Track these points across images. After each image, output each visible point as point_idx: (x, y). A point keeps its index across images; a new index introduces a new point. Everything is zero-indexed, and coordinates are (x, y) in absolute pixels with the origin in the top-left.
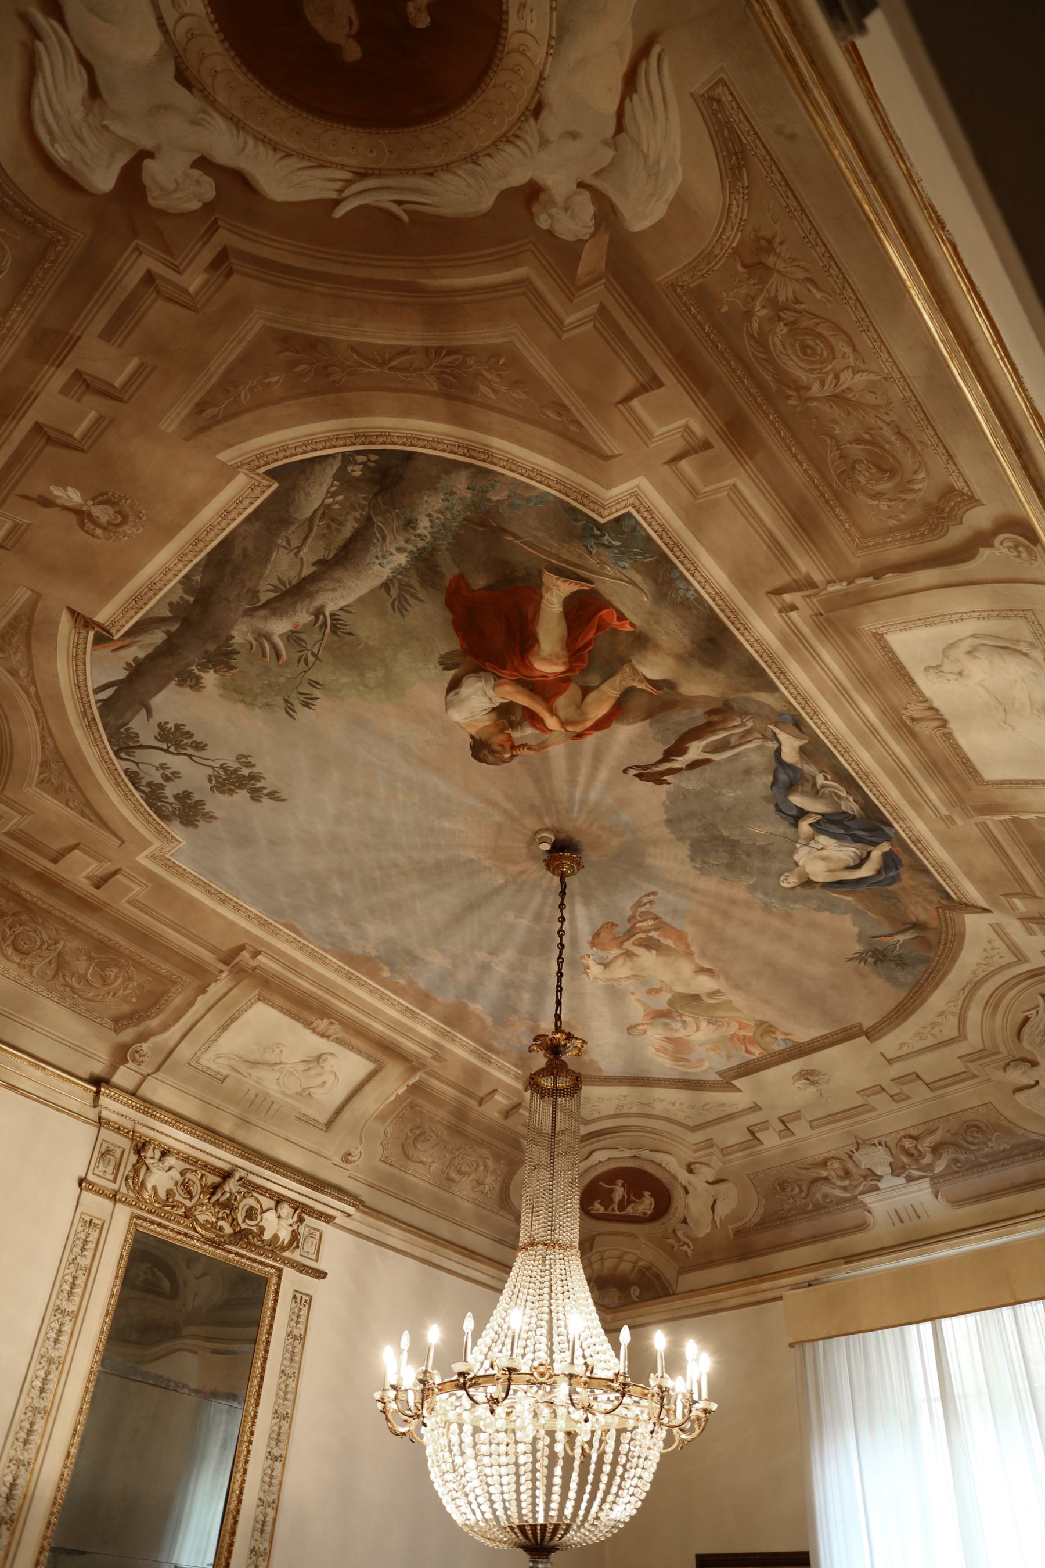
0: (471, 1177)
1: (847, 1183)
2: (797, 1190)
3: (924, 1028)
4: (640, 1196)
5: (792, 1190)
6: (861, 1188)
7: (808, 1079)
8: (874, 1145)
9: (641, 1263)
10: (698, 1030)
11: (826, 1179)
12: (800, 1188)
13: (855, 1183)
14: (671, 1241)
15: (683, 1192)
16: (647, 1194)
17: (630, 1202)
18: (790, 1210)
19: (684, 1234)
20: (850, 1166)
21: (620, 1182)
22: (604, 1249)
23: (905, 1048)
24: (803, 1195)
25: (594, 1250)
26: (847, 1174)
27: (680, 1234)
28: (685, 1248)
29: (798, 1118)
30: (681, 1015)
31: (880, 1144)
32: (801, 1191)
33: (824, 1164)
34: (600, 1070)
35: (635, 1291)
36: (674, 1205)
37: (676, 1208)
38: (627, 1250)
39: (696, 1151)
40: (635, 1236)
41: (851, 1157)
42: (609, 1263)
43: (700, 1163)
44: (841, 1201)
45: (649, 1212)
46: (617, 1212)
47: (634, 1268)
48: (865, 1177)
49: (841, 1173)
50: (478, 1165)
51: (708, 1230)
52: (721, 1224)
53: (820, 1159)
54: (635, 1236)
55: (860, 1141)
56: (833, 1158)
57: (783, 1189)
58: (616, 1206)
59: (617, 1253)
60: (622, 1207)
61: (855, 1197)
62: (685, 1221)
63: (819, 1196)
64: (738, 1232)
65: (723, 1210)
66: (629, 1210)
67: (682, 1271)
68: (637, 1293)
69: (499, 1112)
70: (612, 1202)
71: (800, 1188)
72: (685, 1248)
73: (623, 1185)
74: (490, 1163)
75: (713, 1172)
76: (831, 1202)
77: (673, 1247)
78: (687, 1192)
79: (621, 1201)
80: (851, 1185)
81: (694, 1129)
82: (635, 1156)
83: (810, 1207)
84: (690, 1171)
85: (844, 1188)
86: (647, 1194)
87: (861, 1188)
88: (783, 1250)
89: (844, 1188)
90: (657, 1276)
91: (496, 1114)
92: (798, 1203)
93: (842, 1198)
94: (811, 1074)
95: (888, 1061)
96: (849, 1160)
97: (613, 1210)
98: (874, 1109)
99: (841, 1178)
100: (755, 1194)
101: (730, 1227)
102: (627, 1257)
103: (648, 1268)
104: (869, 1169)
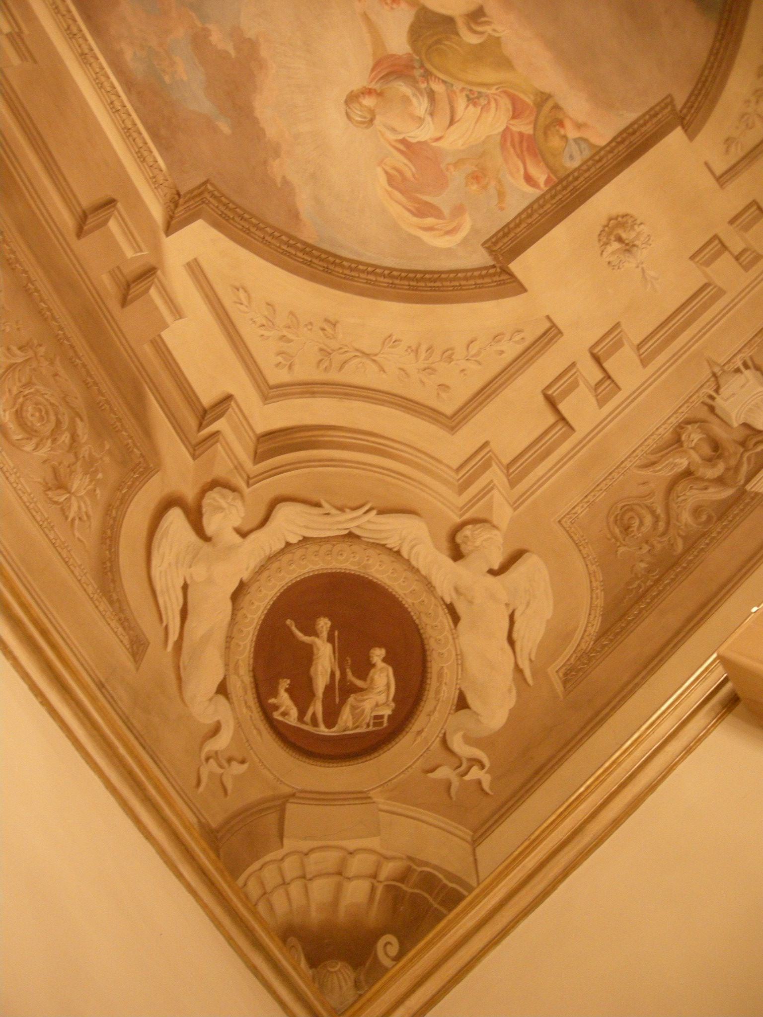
0: (43, 452)
1: (720, 469)
2: (648, 520)
3: (748, 102)
4: (364, 668)
5: (642, 523)
6: (744, 469)
7: (620, 239)
8: (738, 370)
9: (388, 869)
10: (452, 122)
11: (688, 473)
12: (653, 512)
13: (733, 462)
14: (444, 772)
15: (446, 620)
16: (378, 654)
17: (348, 690)
18: (649, 571)
19: (468, 740)
20: (718, 430)
21: (324, 624)
22: (306, 845)
23: (733, 149)
24: (662, 525)
25: (289, 844)
26: (716, 446)
27: (457, 744)
28: (475, 773)
29: (618, 345)
30: (427, 75)
31: (746, 366)
32: (657, 519)
33: (676, 441)
34: (295, 215)
35: (387, 947)
36: (434, 667)
37: (440, 675)
38: (351, 845)
39: (463, 487)
40: (362, 797)
41: (712, 409)
42: (321, 890)
43: (474, 521)
44: (724, 510)
45: (387, 712)
46: (323, 730)
47: (373, 889)
48: (743, 444)
49: (707, 450)
50: (58, 423)
51: (511, 701)
52: (534, 674)
53: (666, 433)
54: (362, 797)
55: (717, 370)
56: (688, 422)
57: (626, 529)
58: (317, 707)
59: (331, 858)
60: (331, 717)
61: (742, 492)
62: (462, 703)
63: (686, 517)
64: (571, 675)
65: (531, 634)
66: (346, 720)
67: (481, 833)
68: (394, 950)
69: (112, 273)
70: (312, 694)
71: (653, 512)
72: (475, 773)
73: (330, 639)
74: (83, 430)
75: (497, 537)
76: (710, 518)
77: (449, 785)
78: (456, 618)
79: (329, 689)
80: (727, 469)
81: (453, 422)
82: (351, 536)
83: (680, 547)
84: (457, 554)
85: (720, 481)
86: (378, 654)
87: (744, 469)
88: (662, 662)
89: (720, 481)
90: (429, 881)
91: (106, 279)
92: (658, 547)
93: (723, 501)
94: (622, 225)
95: (718, 179)
96: (711, 418)
97: (314, 722)
98: (721, 292)
99: (710, 461)
100: (580, 565)
101: (552, 670)
102: (356, 865)
103: (403, 877)
104: (746, 425)
